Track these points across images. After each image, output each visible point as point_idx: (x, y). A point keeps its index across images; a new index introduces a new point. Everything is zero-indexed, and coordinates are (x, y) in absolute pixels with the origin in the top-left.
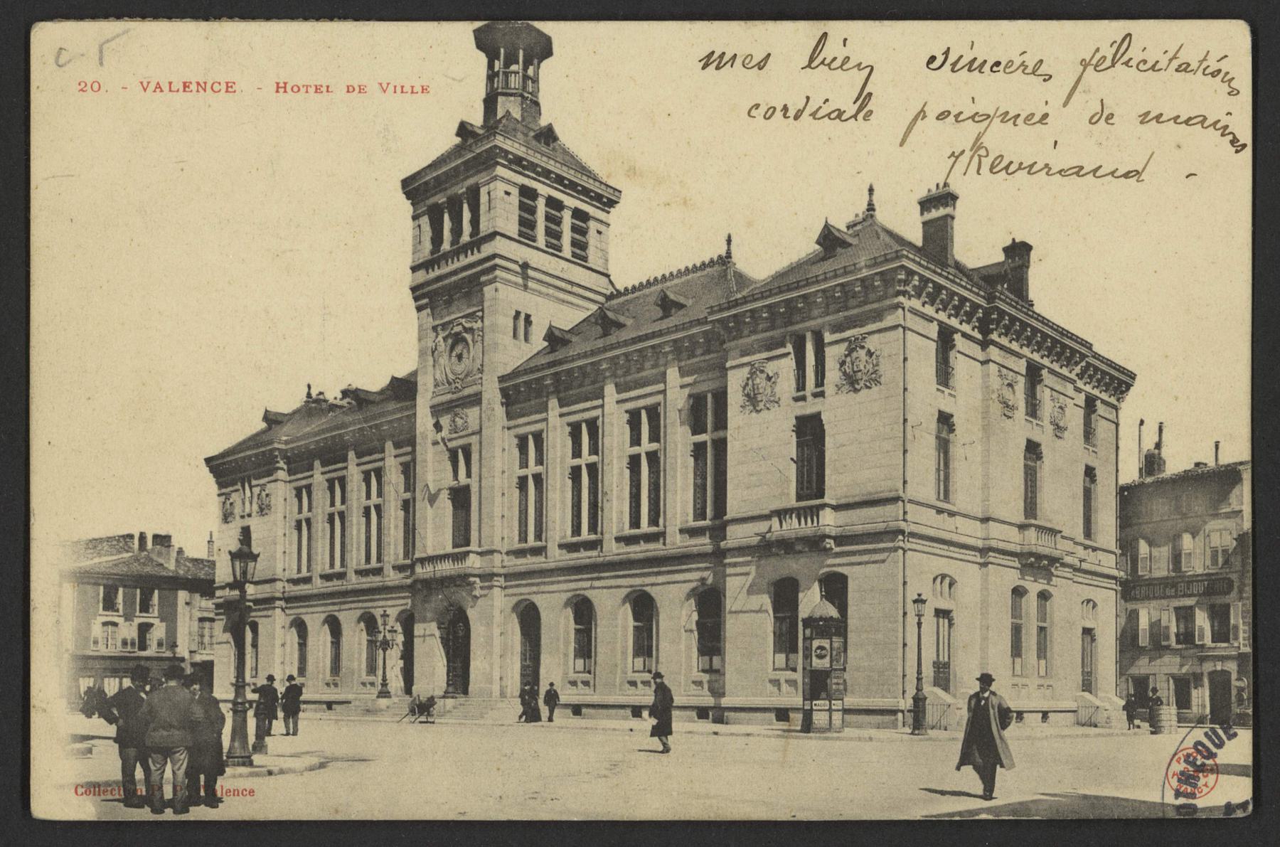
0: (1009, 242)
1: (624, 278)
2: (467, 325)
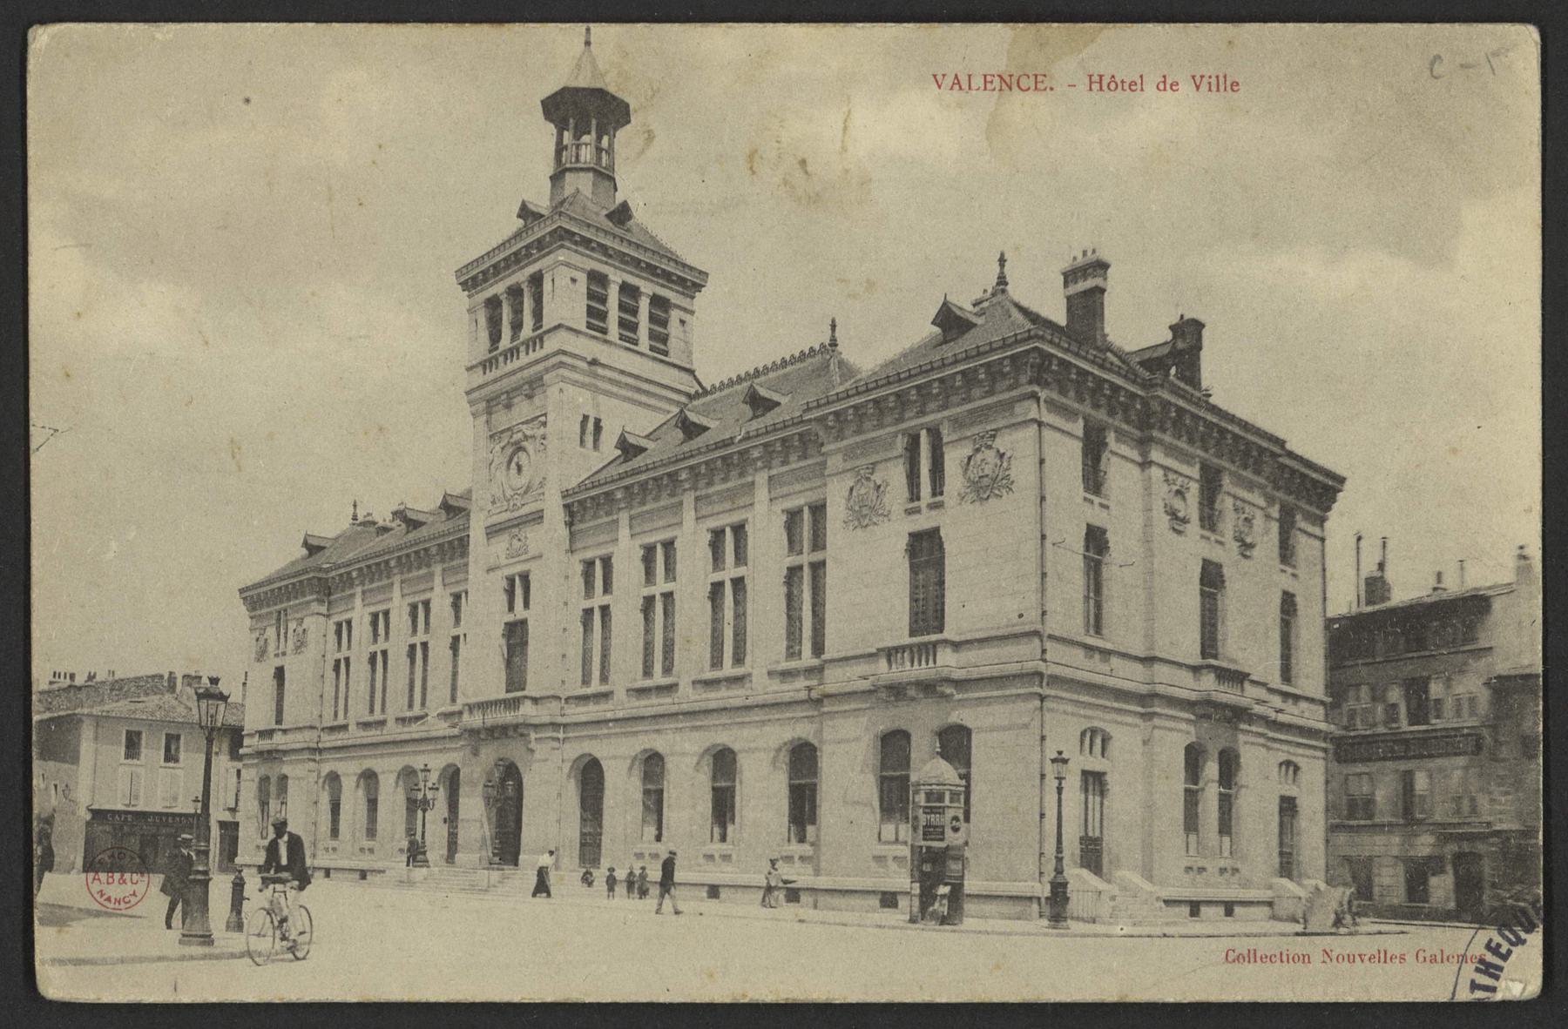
0: (1175, 320)
1: (710, 375)
2: (529, 433)
